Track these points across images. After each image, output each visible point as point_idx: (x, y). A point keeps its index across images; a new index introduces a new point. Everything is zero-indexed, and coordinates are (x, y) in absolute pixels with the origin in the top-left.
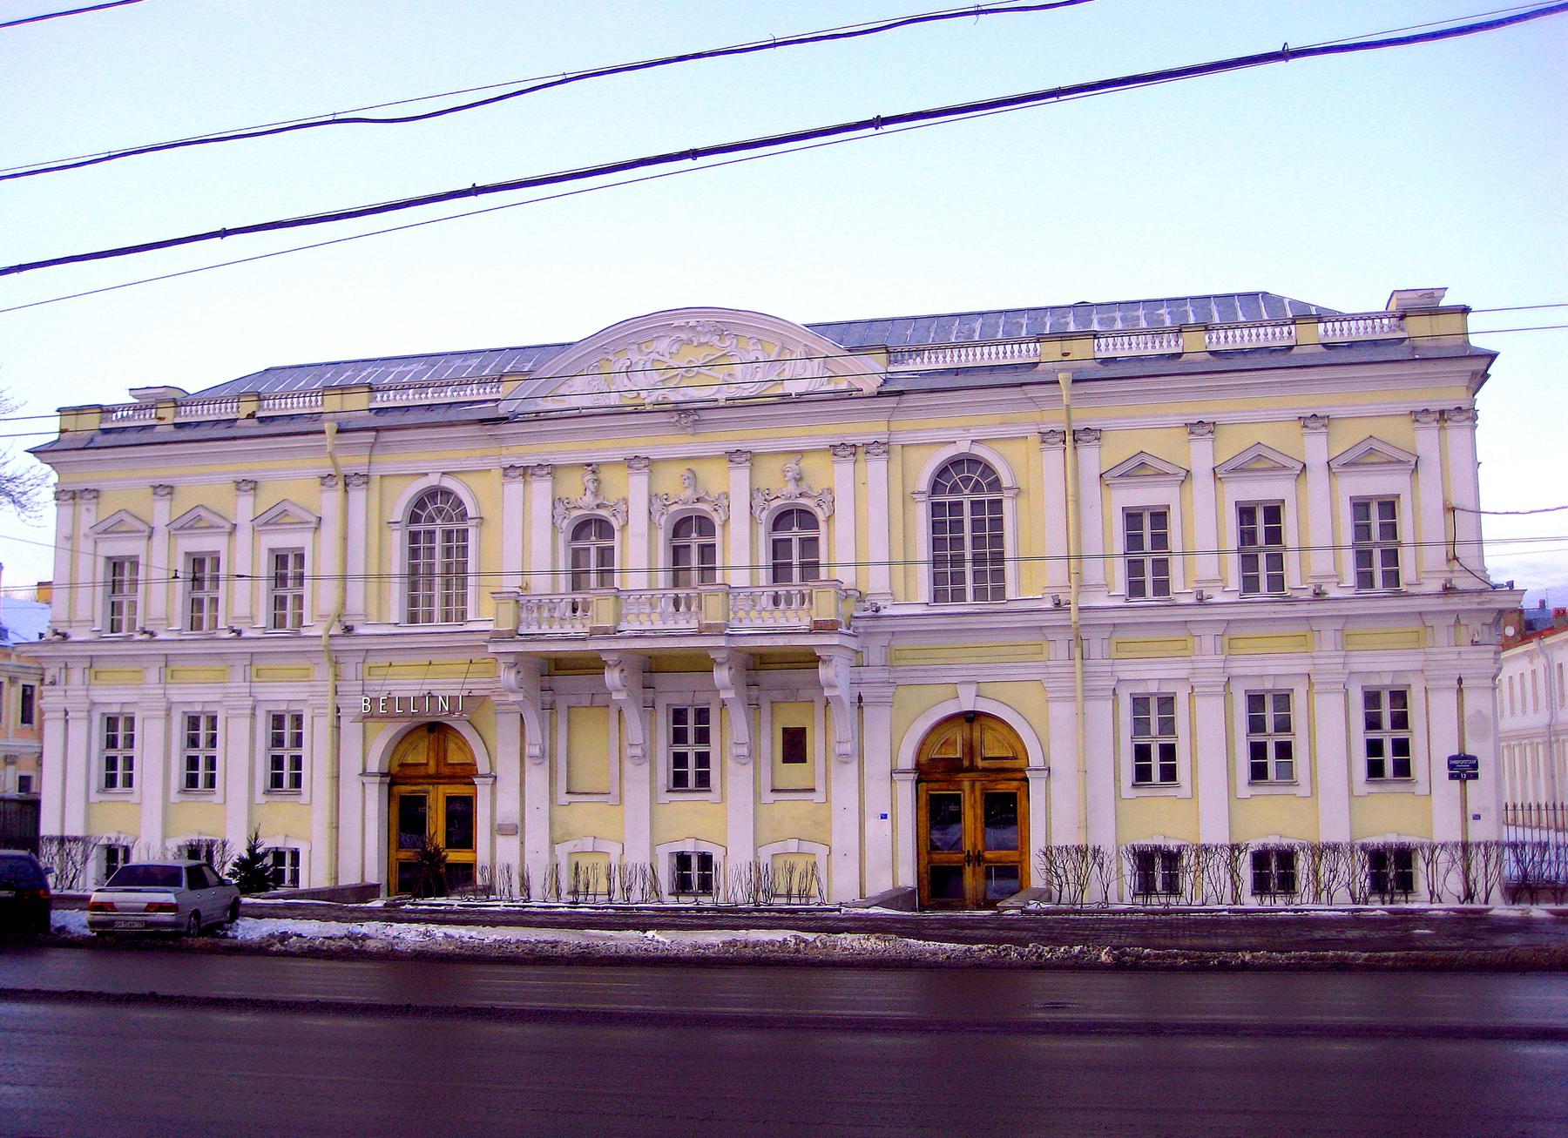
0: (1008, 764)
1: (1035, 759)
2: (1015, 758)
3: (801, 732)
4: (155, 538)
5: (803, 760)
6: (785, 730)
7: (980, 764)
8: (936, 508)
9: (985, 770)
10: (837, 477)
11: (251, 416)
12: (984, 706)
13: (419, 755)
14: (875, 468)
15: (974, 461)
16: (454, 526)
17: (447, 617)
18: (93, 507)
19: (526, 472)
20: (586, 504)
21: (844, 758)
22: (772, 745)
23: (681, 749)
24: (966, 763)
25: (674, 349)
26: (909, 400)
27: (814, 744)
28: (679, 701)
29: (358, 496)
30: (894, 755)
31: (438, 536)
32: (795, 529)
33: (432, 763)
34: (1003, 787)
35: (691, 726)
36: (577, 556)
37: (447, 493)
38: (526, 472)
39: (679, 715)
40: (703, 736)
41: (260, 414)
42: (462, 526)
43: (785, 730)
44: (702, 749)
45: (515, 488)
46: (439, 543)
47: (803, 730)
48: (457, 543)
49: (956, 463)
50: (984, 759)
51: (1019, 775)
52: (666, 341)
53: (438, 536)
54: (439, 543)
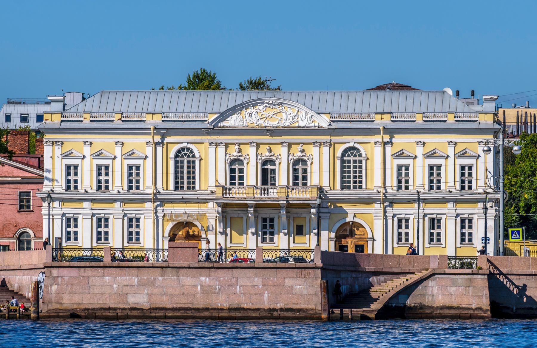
2: (364, 235)
10: (313, 151)
11: (120, 119)
14: (326, 150)
15: (354, 148)
18: (60, 147)
19: (217, 145)
22: (293, 229)
28: (265, 216)
31: (185, 162)
32: (300, 165)
34: (360, 243)
35: (268, 224)
37: (188, 149)
38: (217, 145)
39: (265, 220)
41: (123, 119)
47: (303, 225)
48: (191, 166)
51: (365, 240)
52: (262, 107)
53: (185, 162)
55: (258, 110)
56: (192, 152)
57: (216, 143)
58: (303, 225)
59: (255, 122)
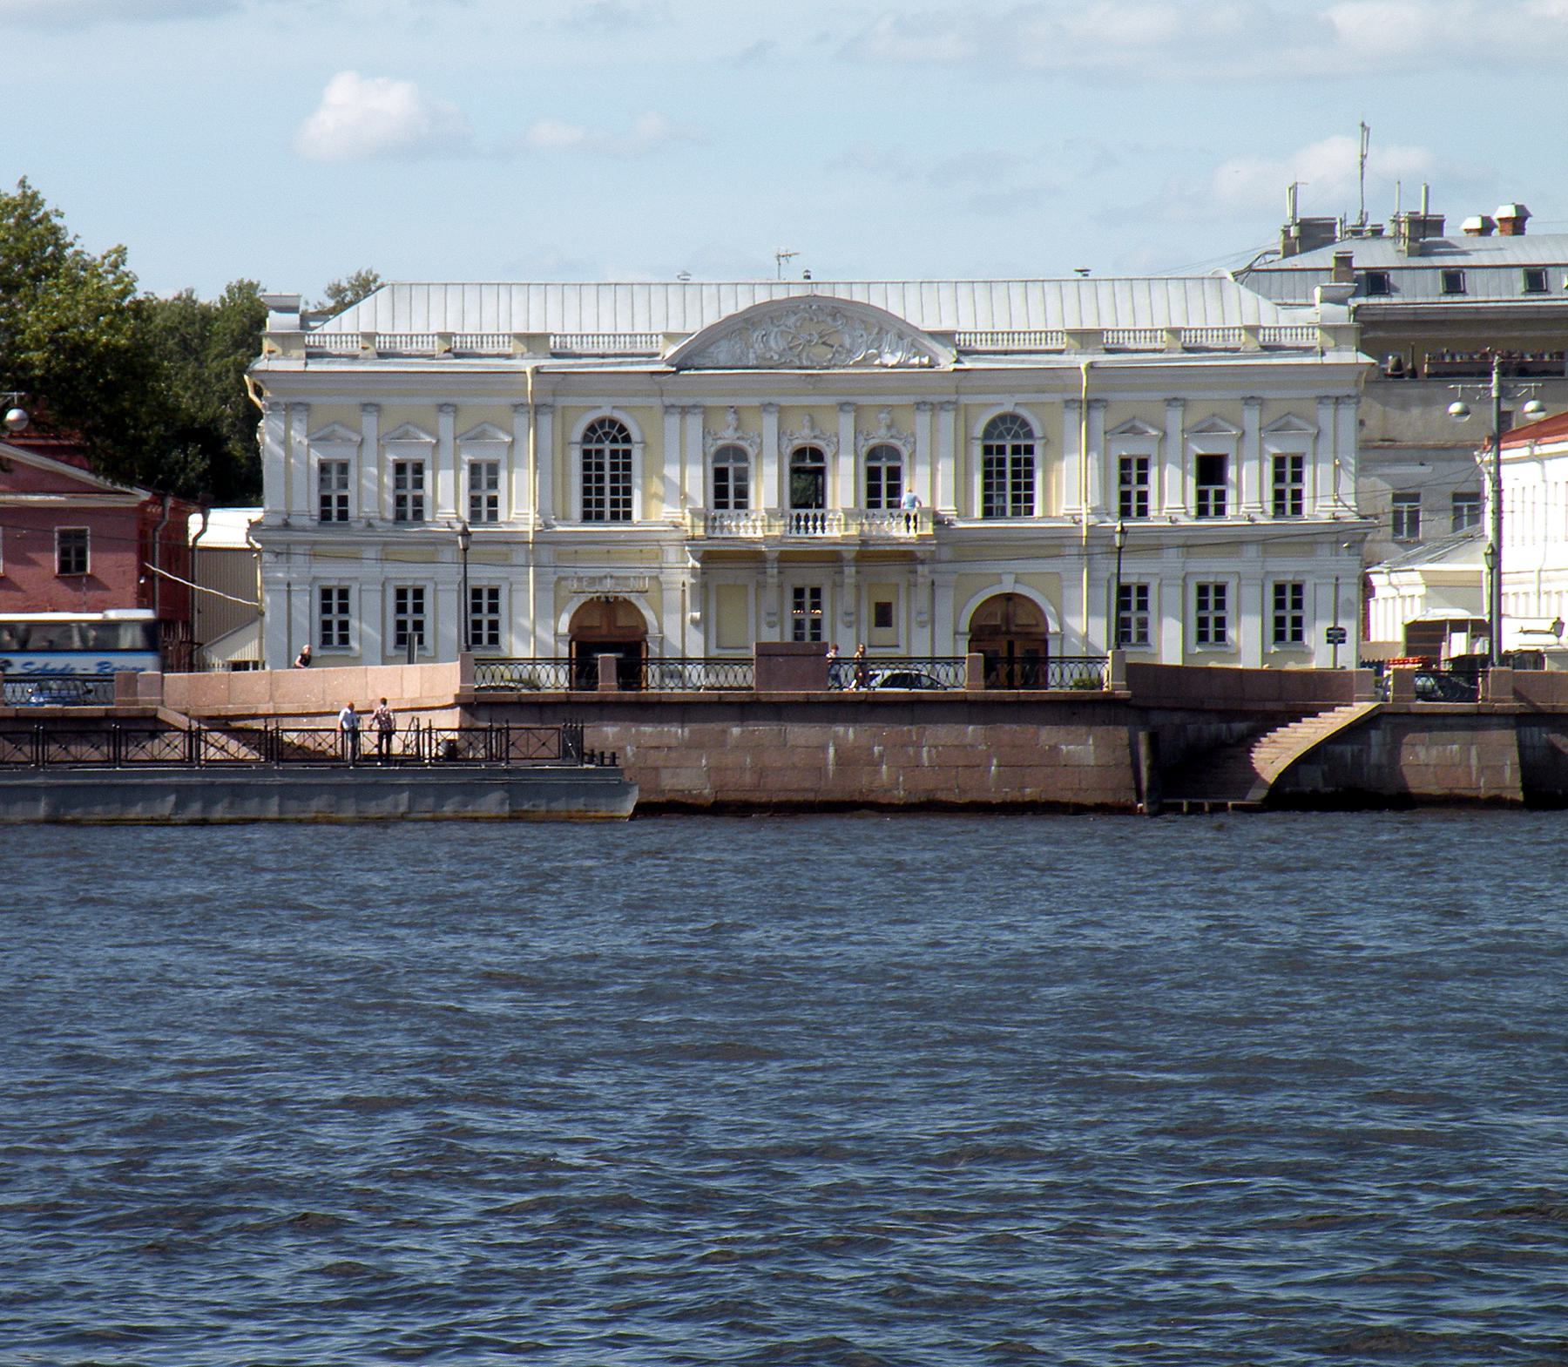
0: (1033, 630)
1: (1053, 627)
4: (365, 447)
5: (889, 625)
6: (878, 605)
7: (1014, 629)
8: (987, 450)
12: (1021, 590)
13: (595, 620)
14: (947, 419)
16: (621, 447)
19: (684, 411)
21: (922, 625)
22: (868, 614)
27: (900, 614)
28: (799, 584)
29: (546, 421)
42: (626, 447)
43: (878, 605)
45: (673, 421)
46: (607, 461)
47: (890, 604)
49: (1002, 418)
54: (607, 461)
56: (622, 429)
57: (683, 408)
58: (890, 604)
59: (776, 357)
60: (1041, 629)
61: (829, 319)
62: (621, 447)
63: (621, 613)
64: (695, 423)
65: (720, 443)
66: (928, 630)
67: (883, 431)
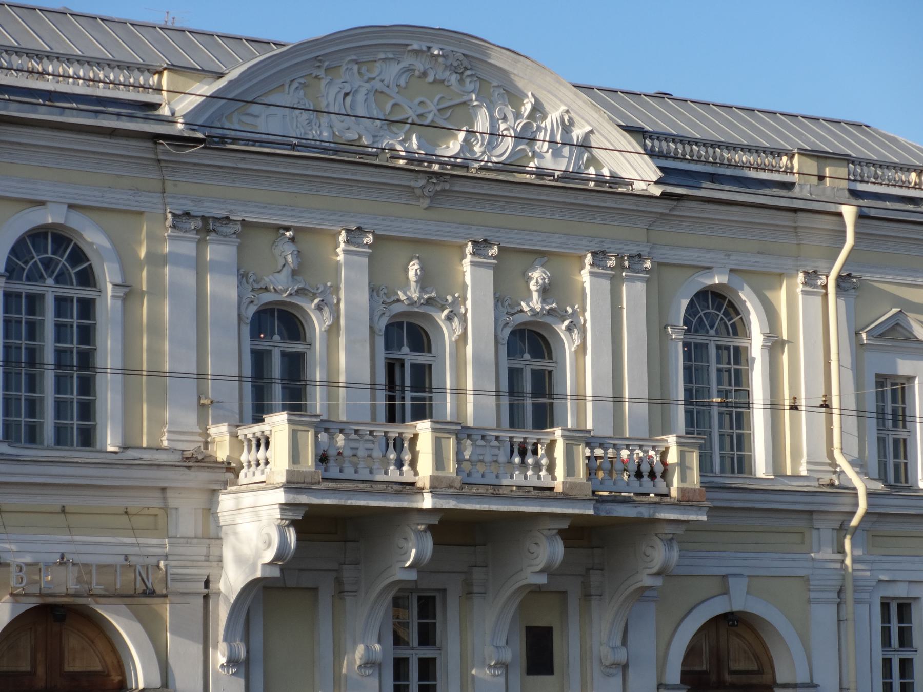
0: (755, 680)
3: (547, 632)
9: (733, 686)
16: (77, 292)
17: (61, 438)
19: (209, 226)
20: (280, 287)
23: (402, 653)
24: (713, 678)
25: (402, 82)
26: (687, 209)
27: (568, 648)
30: (662, 667)
33: (41, 671)
36: (260, 359)
40: (427, 636)
42: (86, 293)
44: (427, 653)
47: (549, 631)
50: (732, 673)
55: (378, 85)
56: (78, 256)
57: (203, 218)
58: (549, 631)
60: (766, 679)
61: (454, 78)
62: (77, 292)
63: (73, 642)
64: (218, 251)
65: (267, 298)
66: (618, 679)
67: (536, 303)
